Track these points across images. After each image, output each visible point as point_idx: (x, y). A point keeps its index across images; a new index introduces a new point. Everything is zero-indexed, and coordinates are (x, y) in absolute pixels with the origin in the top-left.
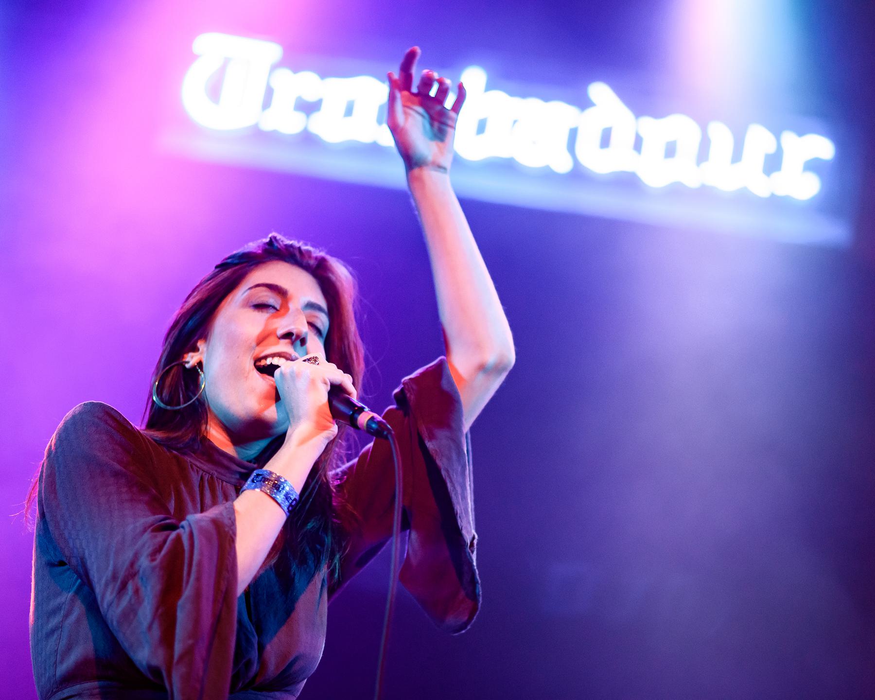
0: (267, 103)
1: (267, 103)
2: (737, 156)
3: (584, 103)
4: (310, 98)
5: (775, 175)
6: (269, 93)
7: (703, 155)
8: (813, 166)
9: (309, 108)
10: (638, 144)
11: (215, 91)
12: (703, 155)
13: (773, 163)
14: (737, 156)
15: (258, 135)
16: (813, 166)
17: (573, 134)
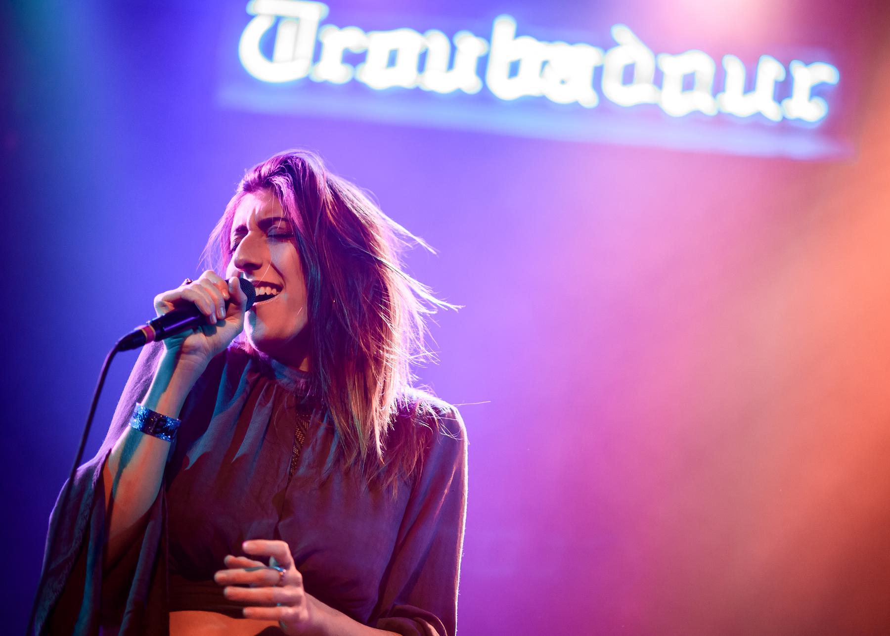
0: (317, 57)
1: (317, 57)
2: (750, 86)
3: (607, 44)
4: (356, 48)
5: (786, 102)
8: (818, 91)
9: (354, 59)
10: (658, 79)
11: (268, 47)
12: (718, 86)
13: (783, 90)
14: (750, 86)
15: (308, 86)
16: (818, 91)
17: (598, 74)
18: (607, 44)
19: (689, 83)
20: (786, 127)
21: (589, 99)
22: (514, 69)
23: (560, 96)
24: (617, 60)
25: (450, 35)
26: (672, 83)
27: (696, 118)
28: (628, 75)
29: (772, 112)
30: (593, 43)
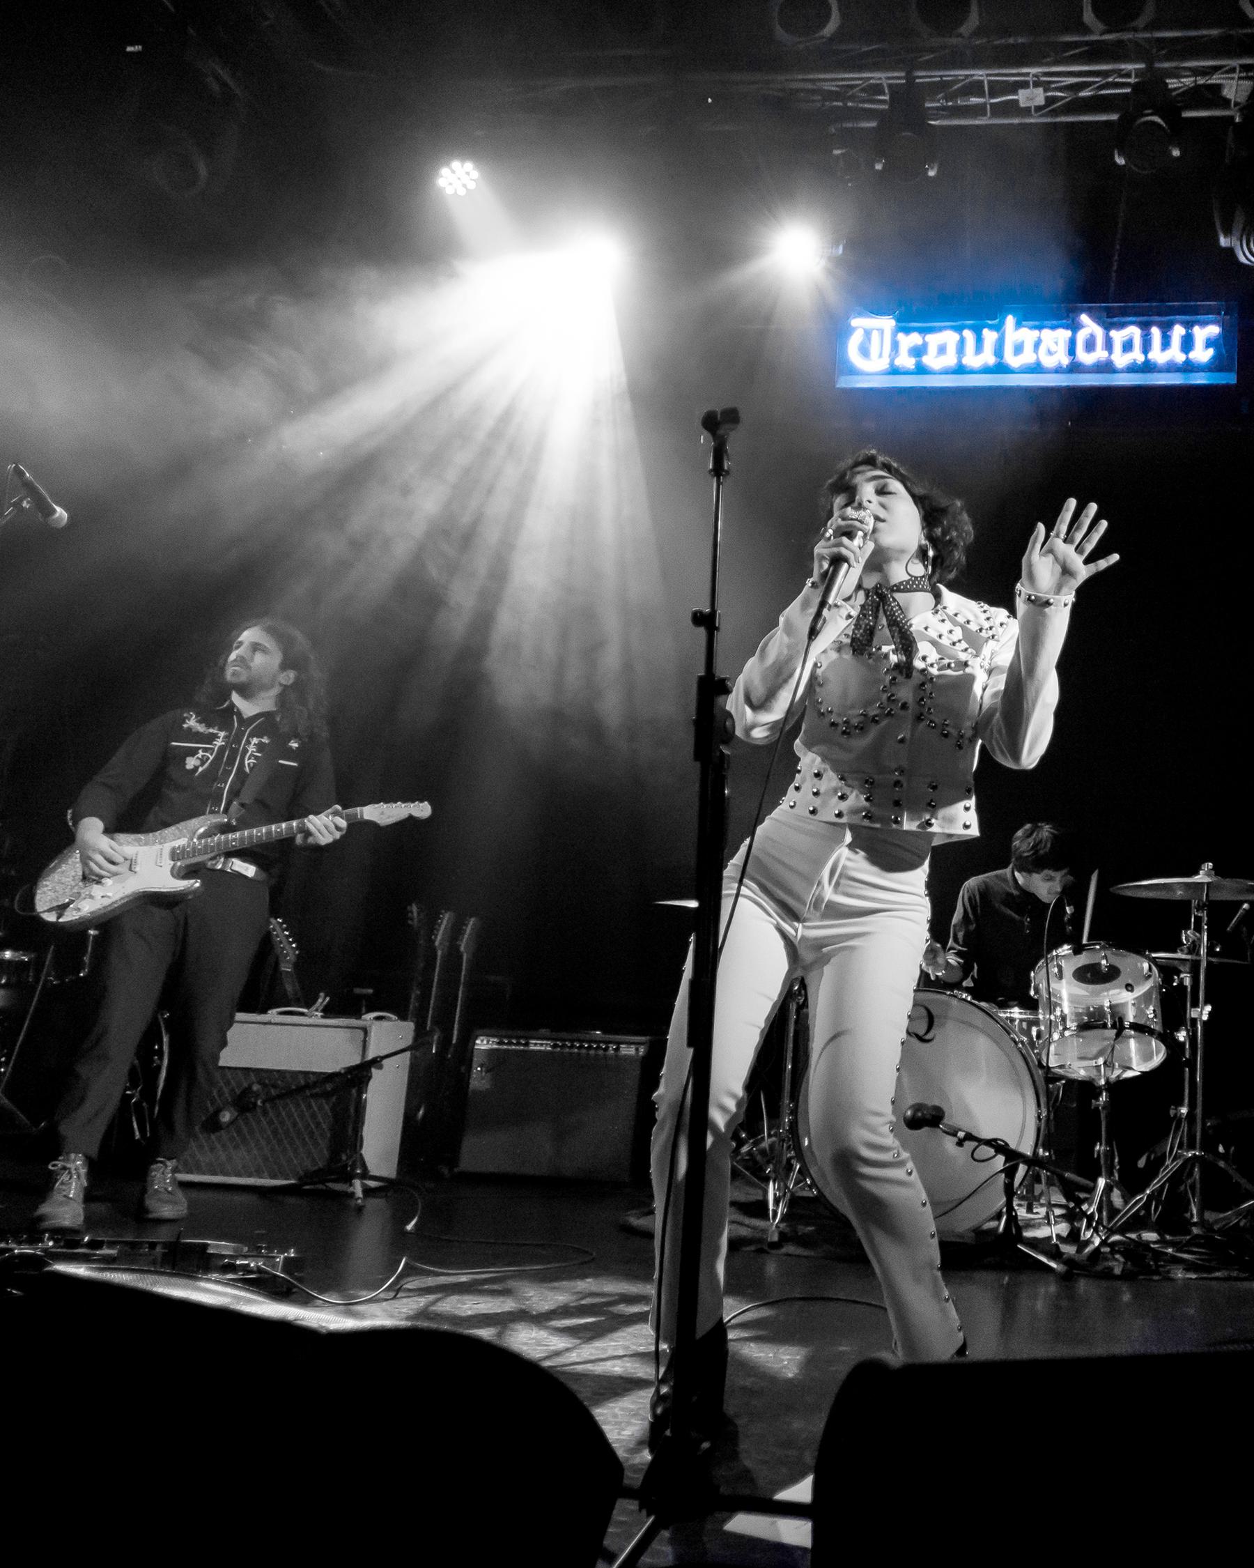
6: (895, 346)
7: (1146, 347)
8: (1209, 343)
9: (918, 352)
10: (1109, 345)
11: (865, 351)
12: (1146, 347)
13: (1187, 343)
16: (1209, 343)
18: (1075, 327)
19: (1128, 347)
20: (1188, 367)
21: (1066, 361)
22: (1018, 349)
23: (1049, 362)
24: (1082, 336)
25: (978, 331)
26: (1118, 347)
27: (1133, 369)
28: (1090, 345)
29: (1180, 358)
30: (1067, 328)
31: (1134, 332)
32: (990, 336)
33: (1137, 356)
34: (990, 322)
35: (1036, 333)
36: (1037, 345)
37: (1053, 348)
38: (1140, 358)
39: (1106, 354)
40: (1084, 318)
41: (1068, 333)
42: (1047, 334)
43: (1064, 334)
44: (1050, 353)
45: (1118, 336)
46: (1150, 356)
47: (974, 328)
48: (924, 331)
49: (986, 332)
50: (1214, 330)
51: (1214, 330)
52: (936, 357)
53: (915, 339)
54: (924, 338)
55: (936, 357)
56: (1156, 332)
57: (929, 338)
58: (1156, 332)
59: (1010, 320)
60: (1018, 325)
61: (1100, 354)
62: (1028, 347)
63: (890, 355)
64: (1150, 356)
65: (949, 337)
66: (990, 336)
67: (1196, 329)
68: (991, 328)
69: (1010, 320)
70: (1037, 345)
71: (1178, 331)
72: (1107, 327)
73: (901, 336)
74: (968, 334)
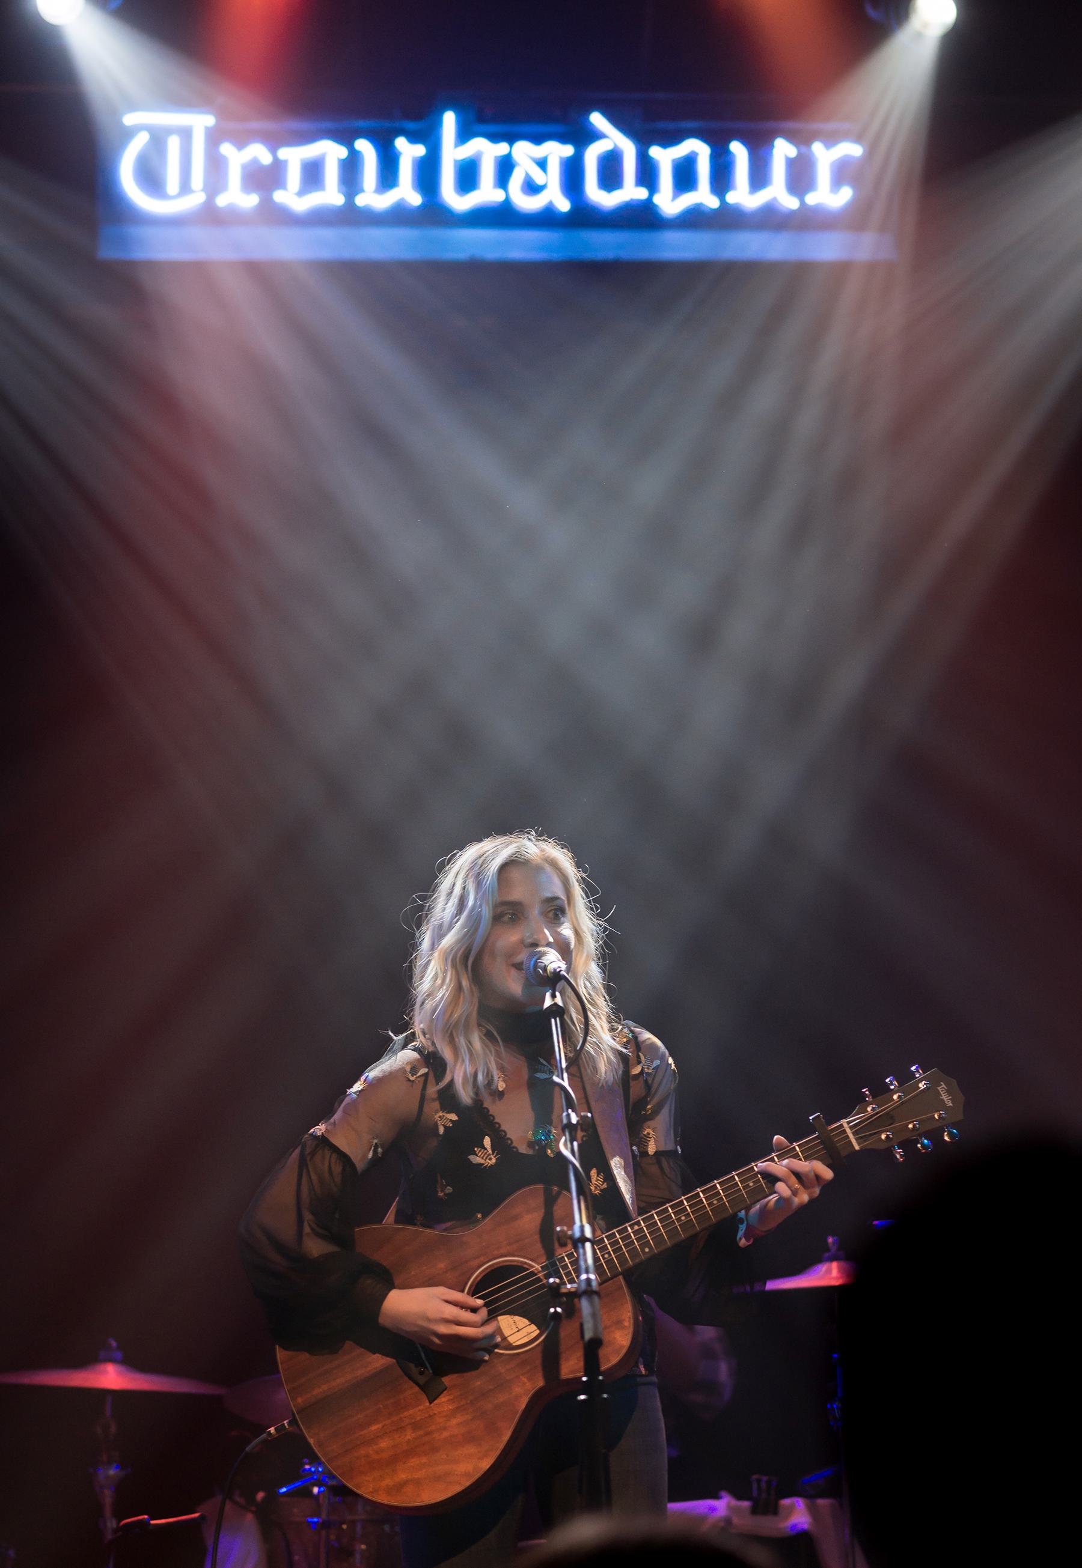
7: (721, 179)
10: (647, 175)
12: (721, 179)
18: (583, 136)
21: (564, 205)
22: (468, 176)
24: (592, 154)
29: (790, 203)
30: (563, 139)
31: (697, 148)
32: (408, 151)
33: (703, 196)
34: (411, 125)
35: (502, 148)
36: (505, 168)
37: (539, 178)
38: (712, 202)
39: (642, 193)
40: (597, 119)
41: (568, 150)
42: (524, 151)
43: (557, 151)
44: (532, 188)
45: (664, 157)
46: (731, 198)
47: (370, 135)
48: (274, 142)
49: (401, 143)
50: (853, 150)
51: (853, 150)
52: (302, 193)
53: (259, 152)
54: (274, 153)
55: (302, 193)
56: (738, 150)
57: (284, 153)
58: (738, 150)
59: (449, 120)
60: (464, 135)
61: (631, 192)
62: (487, 172)
63: (205, 189)
64: (731, 198)
65: (332, 152)
66: (408, 151)
67: (817, 147)
68: (414, 137)
69: (449, 120)
70: (505, 168)
71: (782, 150)
72: (644, 139)
73: (227, 149)
74: (365, 147)
